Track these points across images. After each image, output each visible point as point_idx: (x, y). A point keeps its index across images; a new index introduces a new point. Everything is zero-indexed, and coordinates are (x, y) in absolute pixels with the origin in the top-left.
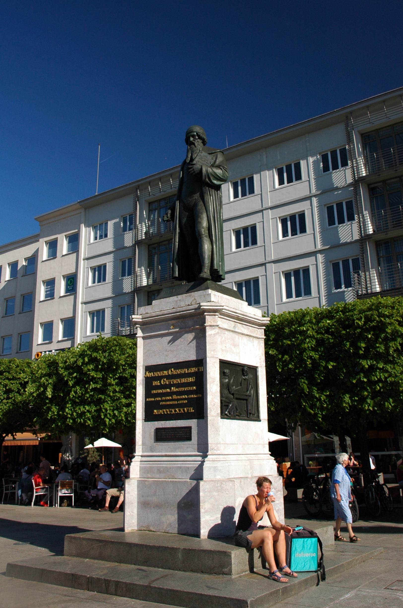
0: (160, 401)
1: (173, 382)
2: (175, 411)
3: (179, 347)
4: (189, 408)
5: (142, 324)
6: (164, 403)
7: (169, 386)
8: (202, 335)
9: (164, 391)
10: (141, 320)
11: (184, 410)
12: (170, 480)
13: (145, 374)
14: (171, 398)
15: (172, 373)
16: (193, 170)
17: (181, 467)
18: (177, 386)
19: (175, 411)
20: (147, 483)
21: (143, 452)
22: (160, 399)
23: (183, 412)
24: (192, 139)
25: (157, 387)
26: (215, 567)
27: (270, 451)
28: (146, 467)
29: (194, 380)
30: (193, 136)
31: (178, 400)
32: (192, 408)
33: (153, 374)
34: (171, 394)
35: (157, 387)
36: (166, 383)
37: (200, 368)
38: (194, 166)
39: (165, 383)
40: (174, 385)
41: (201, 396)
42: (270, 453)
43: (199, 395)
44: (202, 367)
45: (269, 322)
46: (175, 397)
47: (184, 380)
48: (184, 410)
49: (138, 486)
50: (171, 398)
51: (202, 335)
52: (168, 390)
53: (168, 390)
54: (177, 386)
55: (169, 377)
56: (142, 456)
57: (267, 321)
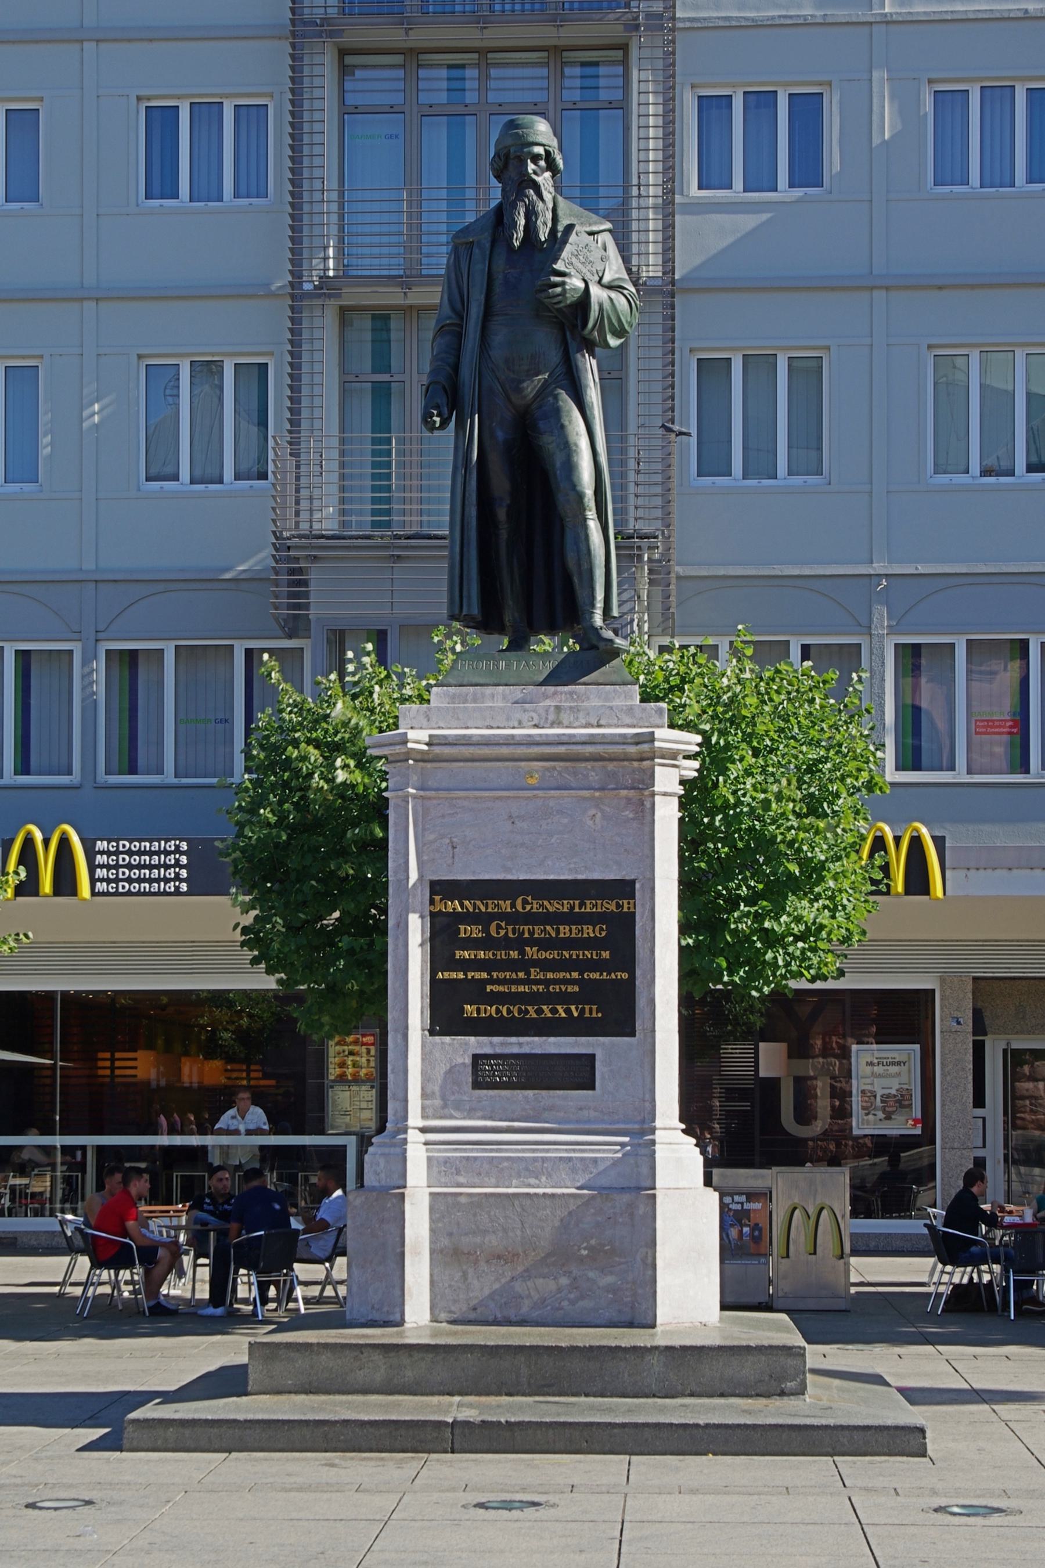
0: (484, 982)
1: (531, 933)
2: (539, 1011)
3: (553, 840)
4: (587, 1007)
5: (419, 757)
6: (496, 988)
7: (520, 944)
8: (631, 816)
9: (501, 955)
10: (426, 748)
11: (568, 1011)
12: (540, 1191)
13: (432, 902)
14: (521, 975)
15: (528, 907)
16: (564, 291)
17: (570, 1159)
18: (544, 944)
19: (539, 1011)
20: (463, 1200)
21: (424, 1117)
22: (484, 975)
23: (563, 1015)
24: (531, 167)
25: (470, 943)
26: (760, 1381)
27: (682, 1120)
28: (449, 1158)
29: (604, 934)
30: (535, 158)
31: (547, 982)
32: (594, 1007)
33: (462, 905)
34: (524, 964)
35: (470, 943)
36: (507, 933)
37: (625, 902)
38: (567, 280)
39: (502, 932)
40: (532, 942)
41: (625, 976)
42: (683, 1126)
43: (619, 974)
44: (632, 901)
45: (696, 774)
46: (535, 973)
47: (570, 930)
48: (568, 1011)
49: (432, 1209)
50: (521, 975)
51: (631, 816)
52: (514, 954)
53: (514, 954)
54: (544, 944)
55: (513, 918)
56: (423, 1130)
57: (691, 769)
